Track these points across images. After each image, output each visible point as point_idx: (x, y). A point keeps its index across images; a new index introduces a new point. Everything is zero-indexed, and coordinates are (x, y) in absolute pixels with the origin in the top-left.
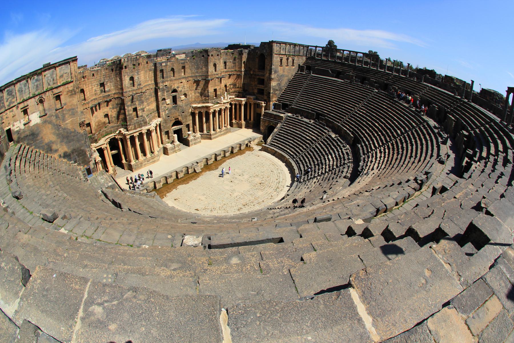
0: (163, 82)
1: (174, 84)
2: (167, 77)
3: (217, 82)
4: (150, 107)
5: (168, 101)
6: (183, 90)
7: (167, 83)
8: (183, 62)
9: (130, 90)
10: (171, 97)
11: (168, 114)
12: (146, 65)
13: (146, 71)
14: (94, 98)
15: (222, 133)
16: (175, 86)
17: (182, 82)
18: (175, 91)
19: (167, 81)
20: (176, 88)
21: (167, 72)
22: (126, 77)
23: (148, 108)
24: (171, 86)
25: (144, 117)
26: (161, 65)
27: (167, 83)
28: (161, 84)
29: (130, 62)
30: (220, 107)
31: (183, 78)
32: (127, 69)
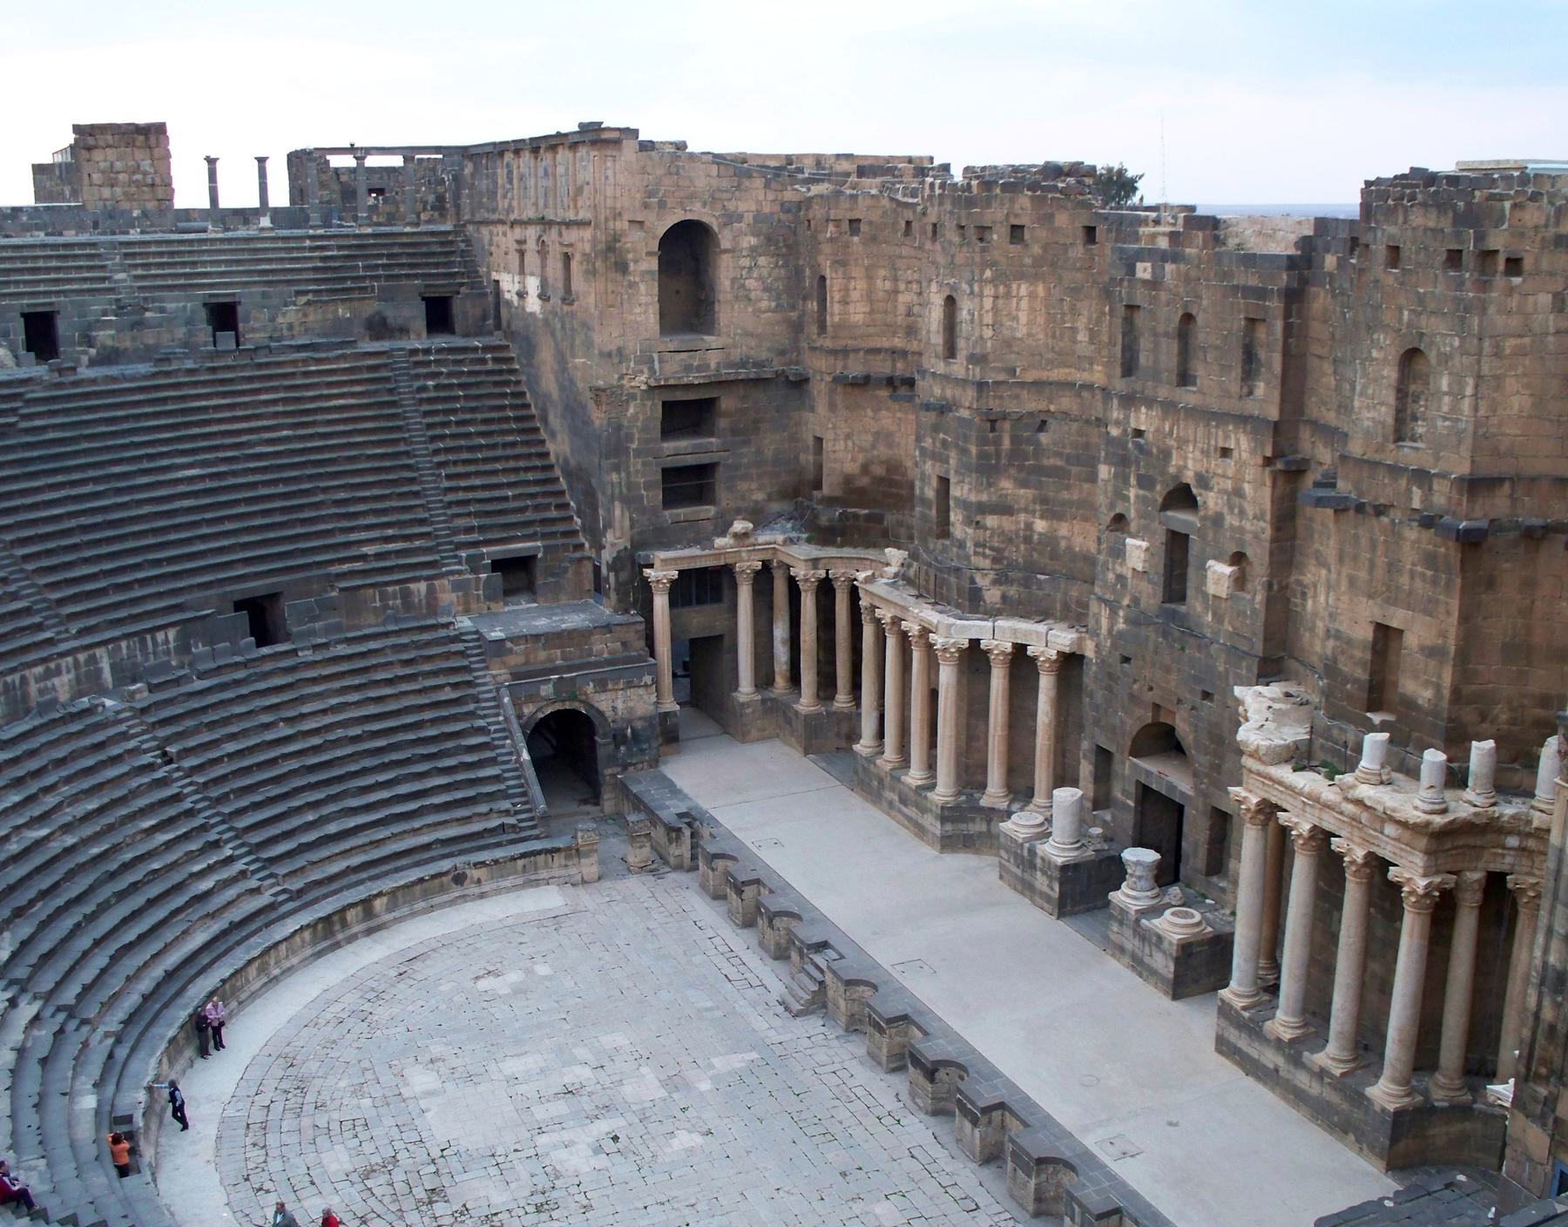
0: (1129, 401)
1: (1182, 442)
2: (1155, 375)
3: (1409, 557)
4: (1063, 529)
5: (1138, 551)
6: (1231, 520)
7: (1143, 419)
8: (1253, 281)
9: (941, 368)
10: (1161, 538)
11: (1121, 634)
12: (1078, 251)
13: (1075, 291)
14: (898, 342)
15: (1303, 1080)
16: (1189, 464)
17: (1226, 452)
18: (1182, 497)
19: (1150, 403)
20: (1189, 477)
21: (1155, 335)
22: (934, 287)
23: (1040, 525)
24: (1166, 454)
25: (968, 558)
26: (1131, 270)
27: (1143, 419)
28: (1116, 414)
29: (948, 207)
30: (1329, 823)
31: (1243, 420)
32: (938, 247)
